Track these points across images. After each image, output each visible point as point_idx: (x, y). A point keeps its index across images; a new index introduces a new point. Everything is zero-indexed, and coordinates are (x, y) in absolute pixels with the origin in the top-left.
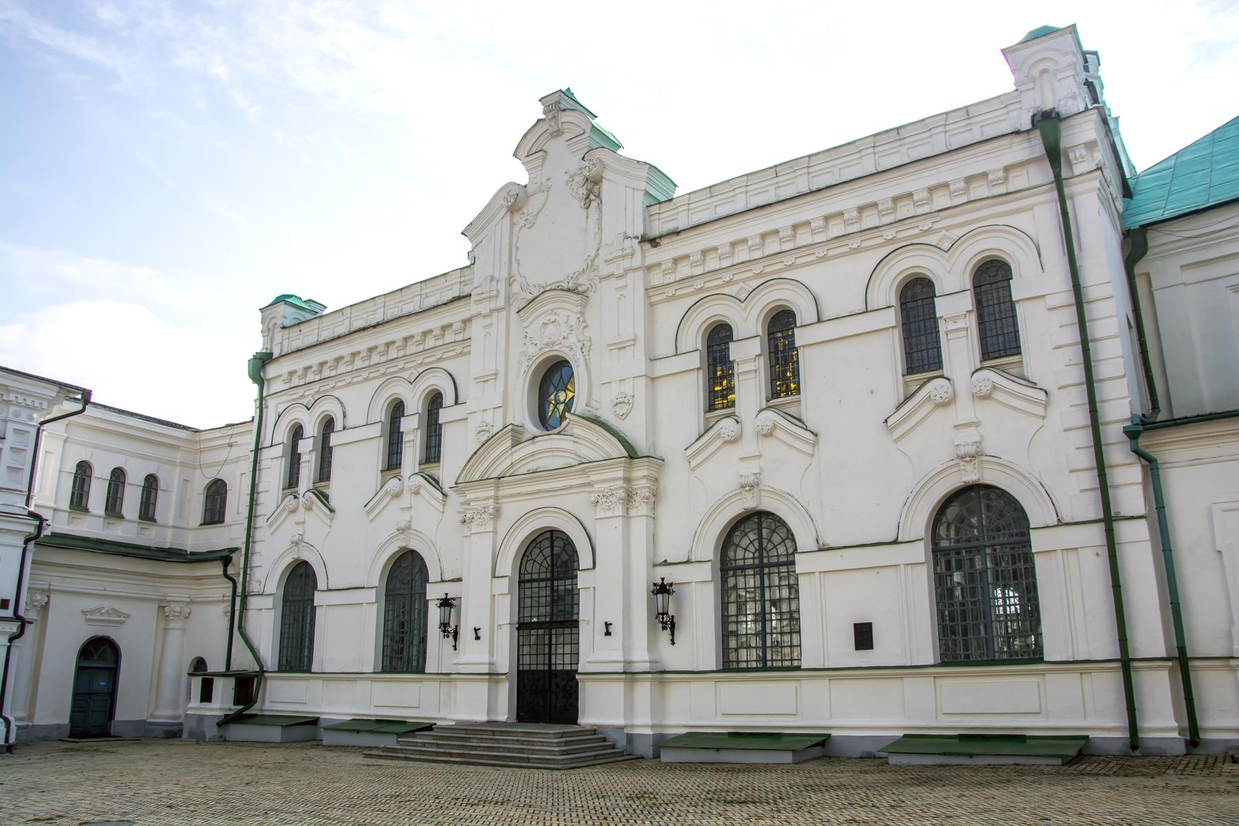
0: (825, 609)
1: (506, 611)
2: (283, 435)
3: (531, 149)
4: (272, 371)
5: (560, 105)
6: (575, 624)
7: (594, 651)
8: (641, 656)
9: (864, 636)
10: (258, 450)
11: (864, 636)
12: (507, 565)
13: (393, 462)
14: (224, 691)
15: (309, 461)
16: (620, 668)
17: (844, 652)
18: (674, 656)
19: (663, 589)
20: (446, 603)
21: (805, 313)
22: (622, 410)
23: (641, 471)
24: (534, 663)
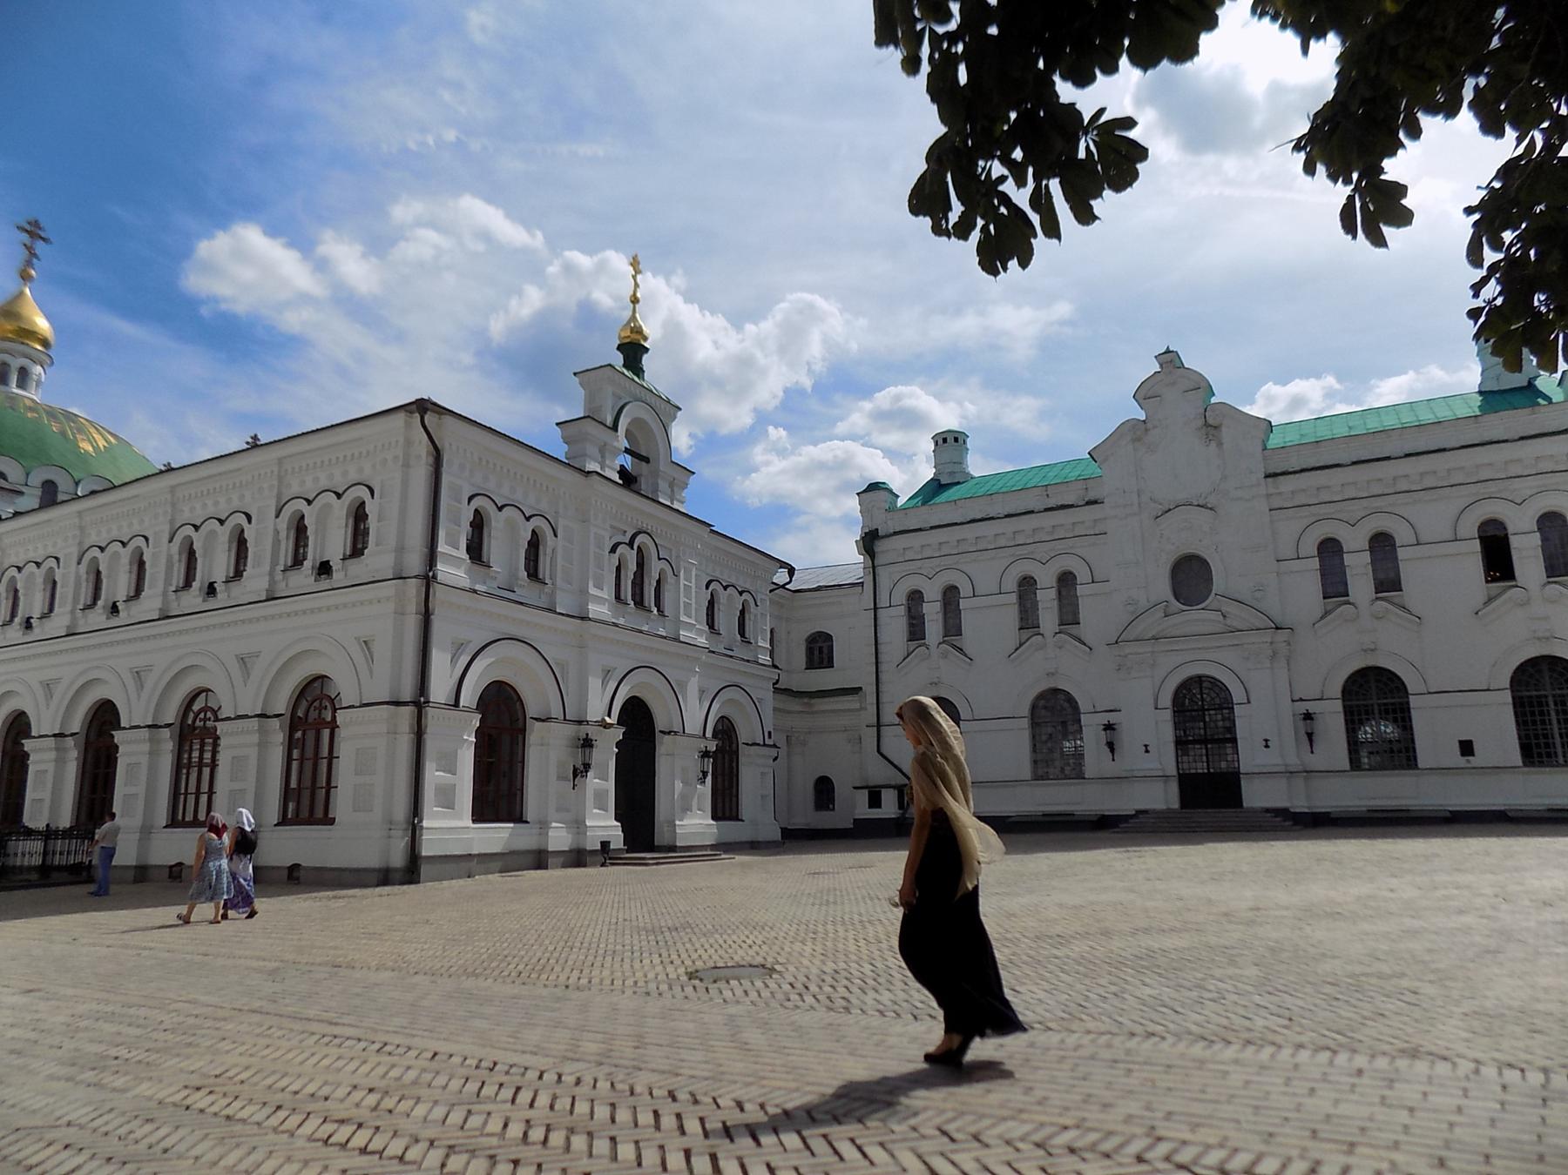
0: (1433, 732)
1: (1168, 733)
2: (900, 597)
3: (1144, 394)
4: (880, 546)
5: (1169, 359)
6: (1234, 741)
7: (1249, 756)
8: (1293, 761)
9: (1467, 748)
10: (875, 609)
11: (1467, 748)
12: (1166, 700)
13: (1028, 620)
14: (889, 799)
15: (936, 618)
16: (1282, 769)
17: (1455, 758)
18: (1317, 761)
19: (1308, 716)
20: (1109, 727)
21: (1402, 534)
22: (1258, 595)
23: (1282, 636)
24: (1201, 768)
